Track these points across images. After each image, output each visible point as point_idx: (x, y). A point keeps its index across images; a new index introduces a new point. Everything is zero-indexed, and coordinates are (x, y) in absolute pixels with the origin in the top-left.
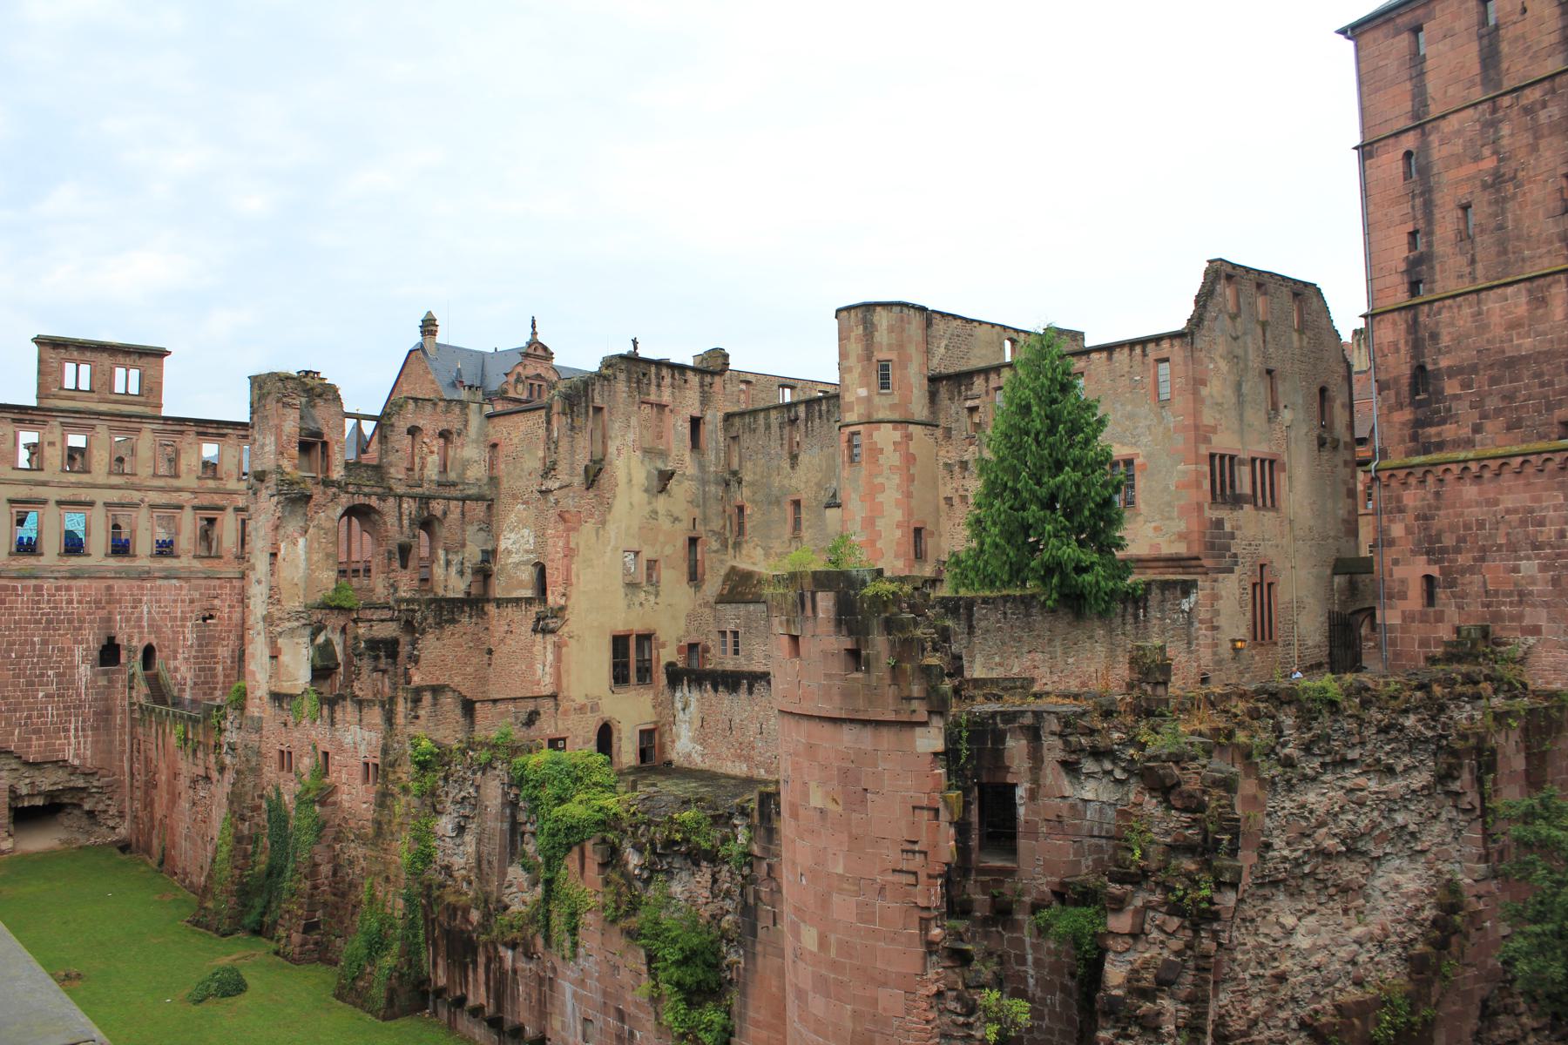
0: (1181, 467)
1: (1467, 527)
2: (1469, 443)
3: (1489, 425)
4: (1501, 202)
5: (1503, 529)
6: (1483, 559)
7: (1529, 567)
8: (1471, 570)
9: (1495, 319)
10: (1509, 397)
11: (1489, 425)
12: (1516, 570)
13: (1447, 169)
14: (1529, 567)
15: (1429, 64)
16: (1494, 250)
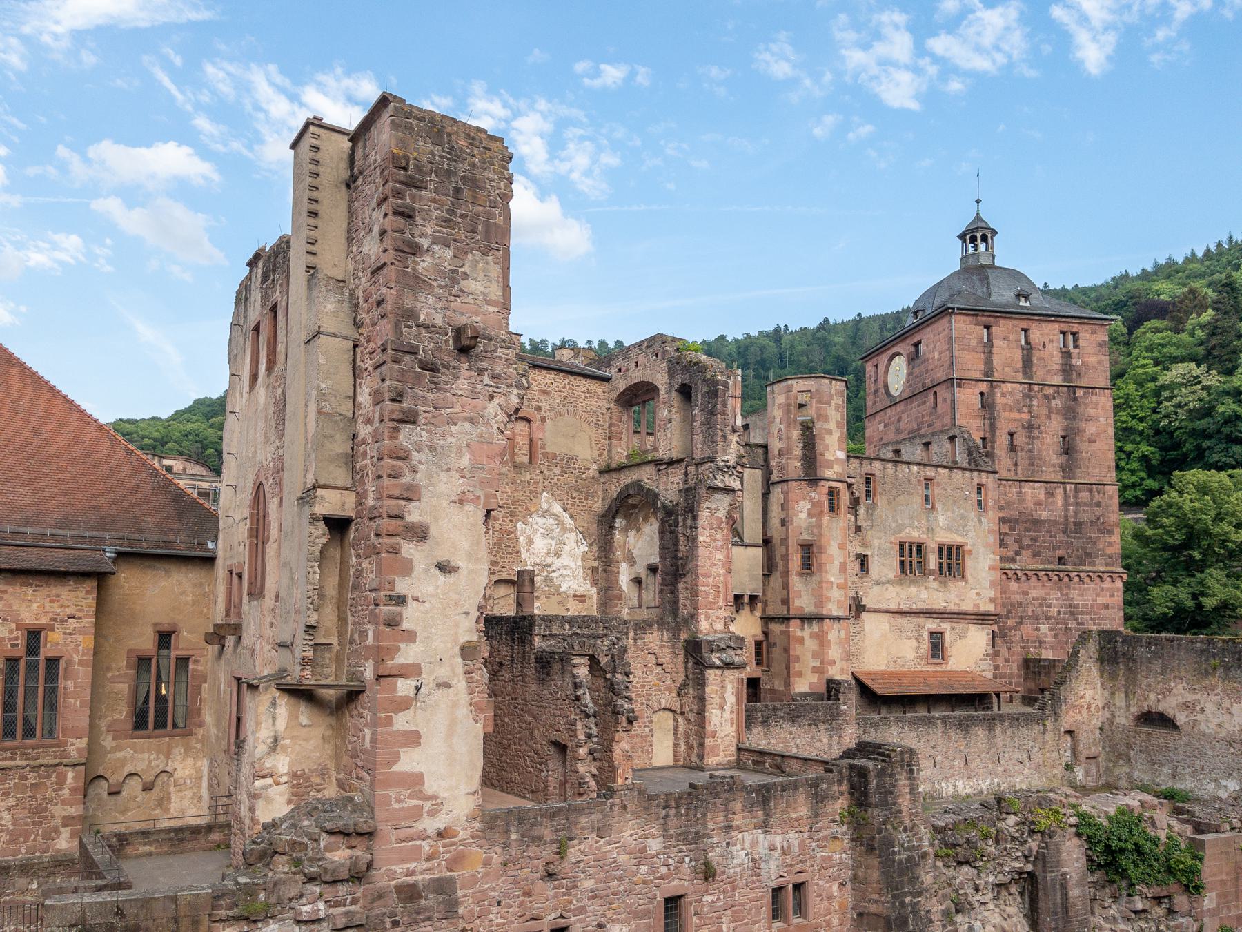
0: (992, 556)
1: (1012, 605)
2: (1013, 560)
3: (1024, 552)
4: (1031, 438)
5: (1030, 609)
6: (1021, 623)
7: (1044, 628)
8: (1015, 629)
9: (1029, 498)
10: (1035, 540)
11: (1024, 552)
12: (1038, 629)
13: (1004, 410)
14: (1044, 628)
15: (995, 350)
16: (1027, 462)
